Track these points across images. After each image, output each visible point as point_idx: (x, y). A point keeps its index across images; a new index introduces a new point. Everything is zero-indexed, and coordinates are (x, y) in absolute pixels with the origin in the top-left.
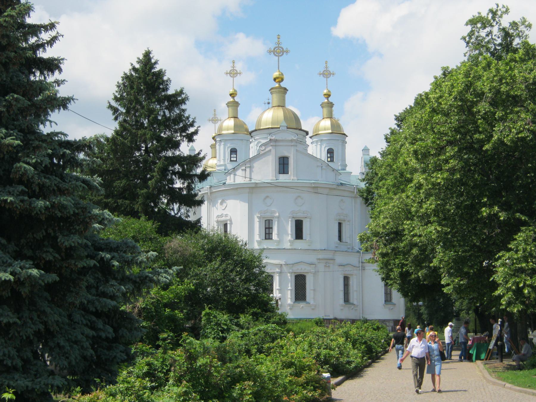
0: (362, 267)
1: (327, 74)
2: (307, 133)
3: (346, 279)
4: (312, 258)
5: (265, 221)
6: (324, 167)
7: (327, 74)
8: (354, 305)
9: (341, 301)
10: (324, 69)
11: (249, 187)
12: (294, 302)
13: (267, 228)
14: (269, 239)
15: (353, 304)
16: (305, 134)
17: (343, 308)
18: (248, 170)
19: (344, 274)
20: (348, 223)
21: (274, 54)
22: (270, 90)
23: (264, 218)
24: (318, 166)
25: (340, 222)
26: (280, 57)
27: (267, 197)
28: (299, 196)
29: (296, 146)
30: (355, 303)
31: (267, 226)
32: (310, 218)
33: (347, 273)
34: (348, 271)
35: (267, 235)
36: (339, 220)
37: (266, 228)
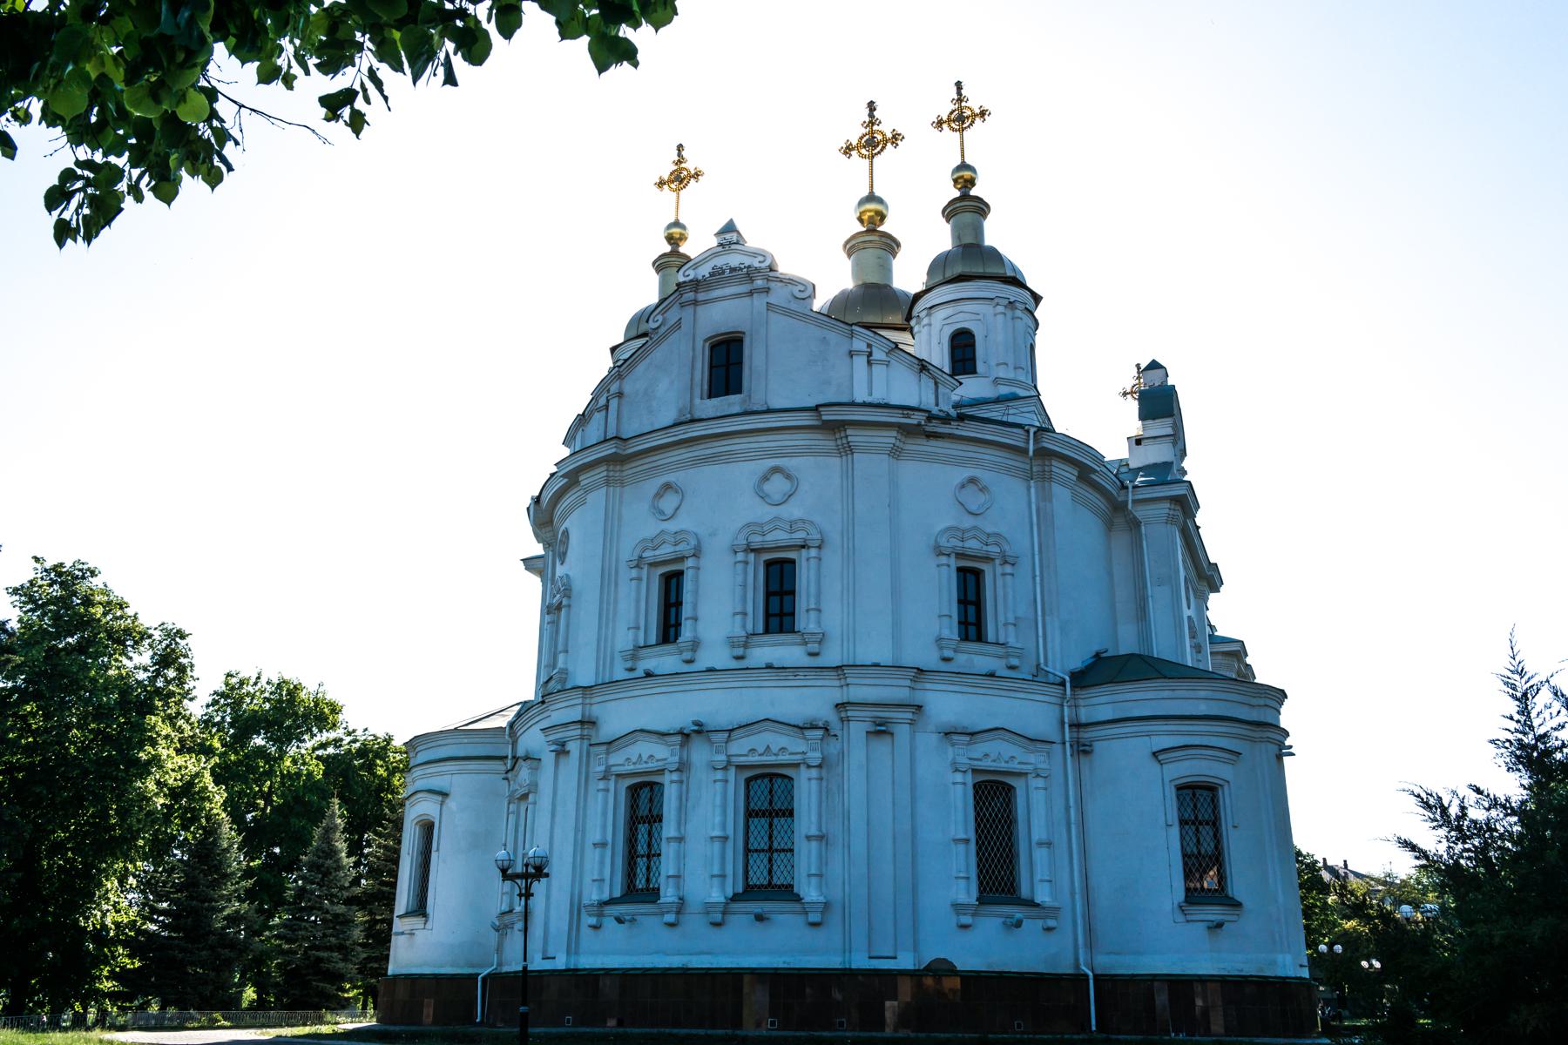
4: (814, 701)
6: (878, 354)
8: (1038, 905)
9: (967, 892)
10: (953, 107)
15: (1031, 903)
17: (966, 920)
18: (614, 404)
20: (1008, 569)
27: (668, 487)
28: (776, 470)
30: (1043, 896)
32: (819, 547)
34: (998, 755)
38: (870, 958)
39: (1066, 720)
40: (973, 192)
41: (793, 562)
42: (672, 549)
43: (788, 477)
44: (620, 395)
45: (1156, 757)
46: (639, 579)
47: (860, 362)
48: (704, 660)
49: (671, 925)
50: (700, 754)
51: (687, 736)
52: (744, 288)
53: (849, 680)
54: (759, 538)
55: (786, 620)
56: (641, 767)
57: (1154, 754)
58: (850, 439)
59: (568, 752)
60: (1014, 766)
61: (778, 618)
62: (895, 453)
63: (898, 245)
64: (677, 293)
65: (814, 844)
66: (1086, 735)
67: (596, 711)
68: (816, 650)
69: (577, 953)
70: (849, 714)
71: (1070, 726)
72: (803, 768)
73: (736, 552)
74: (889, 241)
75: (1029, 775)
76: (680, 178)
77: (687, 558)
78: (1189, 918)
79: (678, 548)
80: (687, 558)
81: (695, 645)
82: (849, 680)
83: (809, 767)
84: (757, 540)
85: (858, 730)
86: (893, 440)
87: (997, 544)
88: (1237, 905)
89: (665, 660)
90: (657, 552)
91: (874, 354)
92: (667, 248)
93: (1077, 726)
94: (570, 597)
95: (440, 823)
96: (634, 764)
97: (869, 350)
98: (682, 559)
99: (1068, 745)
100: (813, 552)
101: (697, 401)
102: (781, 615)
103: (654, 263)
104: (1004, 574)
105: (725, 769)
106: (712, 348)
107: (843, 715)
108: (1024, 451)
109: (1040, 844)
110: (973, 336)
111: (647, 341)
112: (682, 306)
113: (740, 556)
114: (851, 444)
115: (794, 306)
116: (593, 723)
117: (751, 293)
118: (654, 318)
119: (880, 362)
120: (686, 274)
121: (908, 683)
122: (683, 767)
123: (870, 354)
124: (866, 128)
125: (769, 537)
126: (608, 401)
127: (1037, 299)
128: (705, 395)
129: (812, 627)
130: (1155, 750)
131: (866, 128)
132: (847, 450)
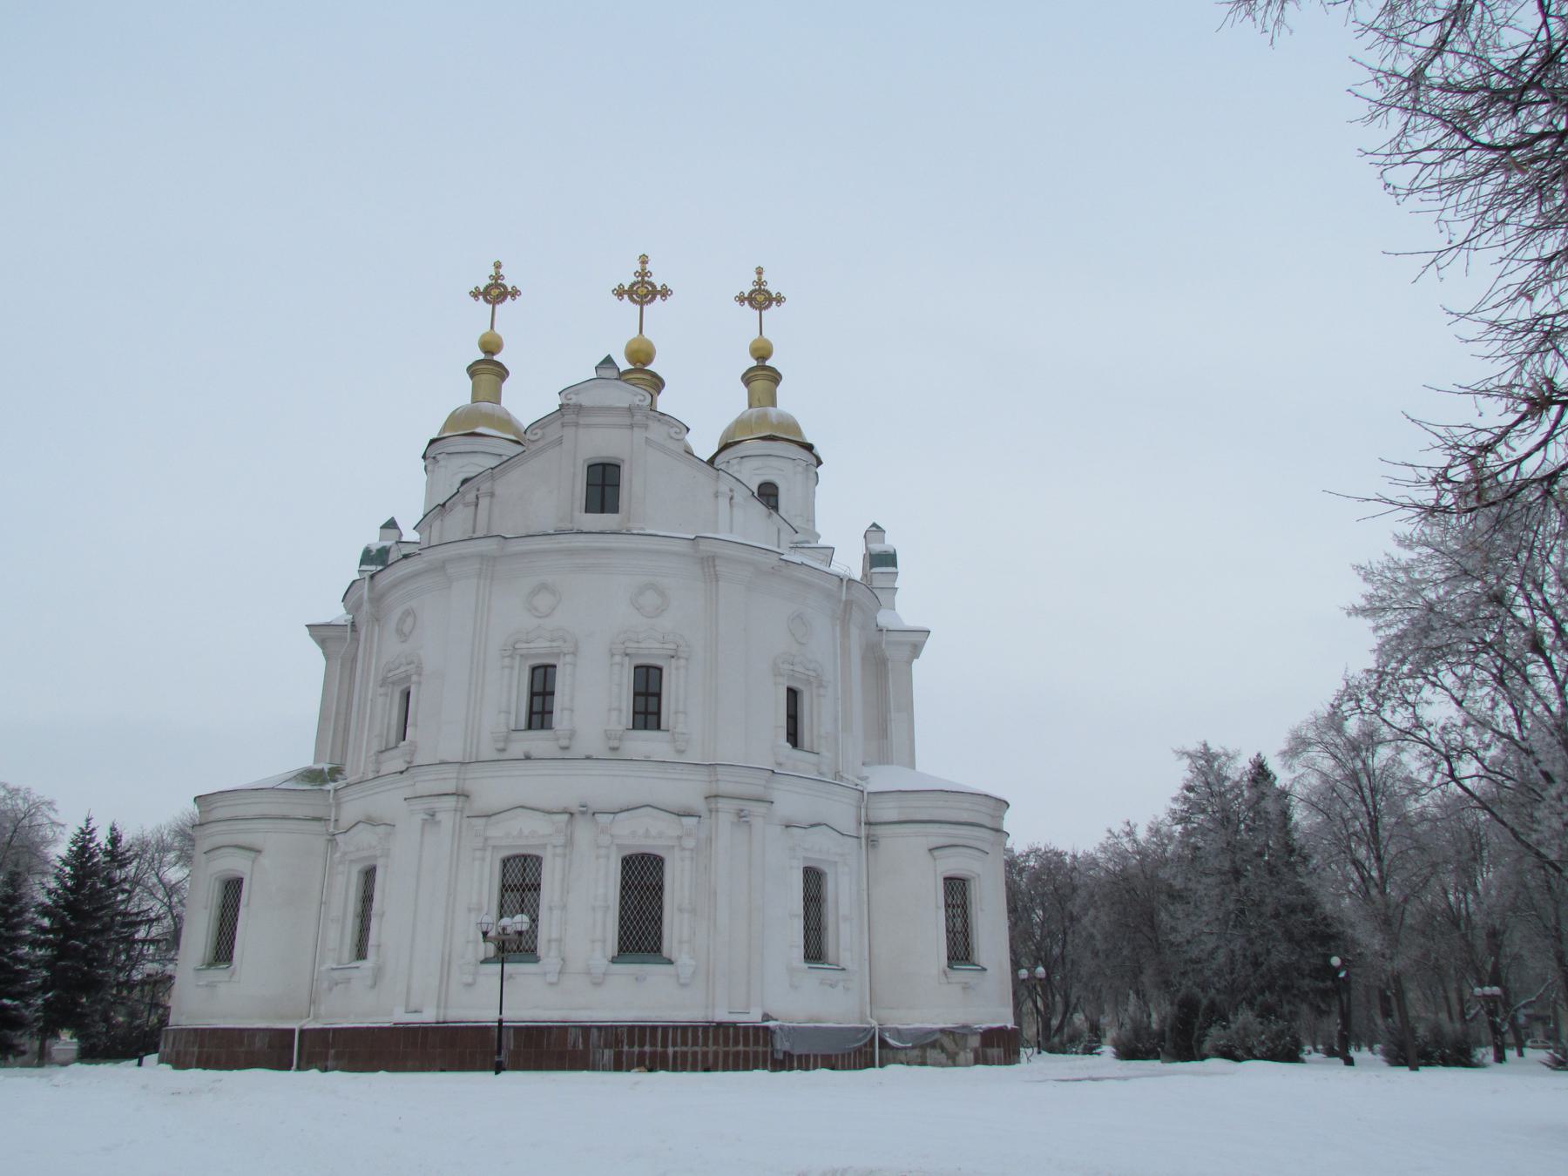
0: (867, 837)
1: (760, 298)
3: (813, 880)
4: (689, 791)
6: (738, 499)
7: (760, 298)
11: (482, 557)
12: (614, 961)
13: (538, 694)
18: (484, 502)
19: (805, 858)
25: (794, 685)
27: (543, 587)
29: (646, 427)
31: (538, 688)
32: (687, 659)
34: (821, 848)
37: (533, 694)
38: (730, 1013)
39: (863, 819)
40: (768, 363)
41: (660, 669)
42: (548, 644)
44: (492, 495)
45: (931, 854)
46: (512, 668)
47: (723, 503)
48: (580, 749)
49: (551, 984)
50: (584, 832)
51: (572, 814)
54: (636, 645)
55: (652, 719)
57: (930, 850)
59: (440, 822)
61: (643, 716)
63: (663, 385)
64: (559, 413)
66: (879, 830)
67: (469, 786)
68: (683, 748)
69: (446, 1007)
71: (866, 824)
73: (613, 655)
74: (657, 381)
76: (496, 292)
78: (950, 981)
79: (554, 644)
80: (565, 654)
81: (572, 735)
82: (719, 777)
83: (683, 849)
85: (725, 819)
88: (984, 969)
89: (538, 741)
90: (532, 645)
91: (735, 497)
92: (482, 356)
93: (868, 824)
94: (420, 675)
95: (251, 879)
98: (558, 655)
99: (863, 840)
100: (682, 662)
101: (577, 514)
102: (646, 713)
103: (469, 368)
105: (608, 847)
106: (589, 467)
107: (713, 806)
110: (777, 488)
111: (524, 451)
112: (563, 425)
113: (617, 659)
116: (467, 796)
118: (534, 430)
120: (569, 397)
122: (569, 843)
123: (731, 498)
124: (637, 277)
125: (642, 645)
126: (477, 498)
127: (819, 463)
128: (584, 510)
130: (931, 847)
131: (637, 277)
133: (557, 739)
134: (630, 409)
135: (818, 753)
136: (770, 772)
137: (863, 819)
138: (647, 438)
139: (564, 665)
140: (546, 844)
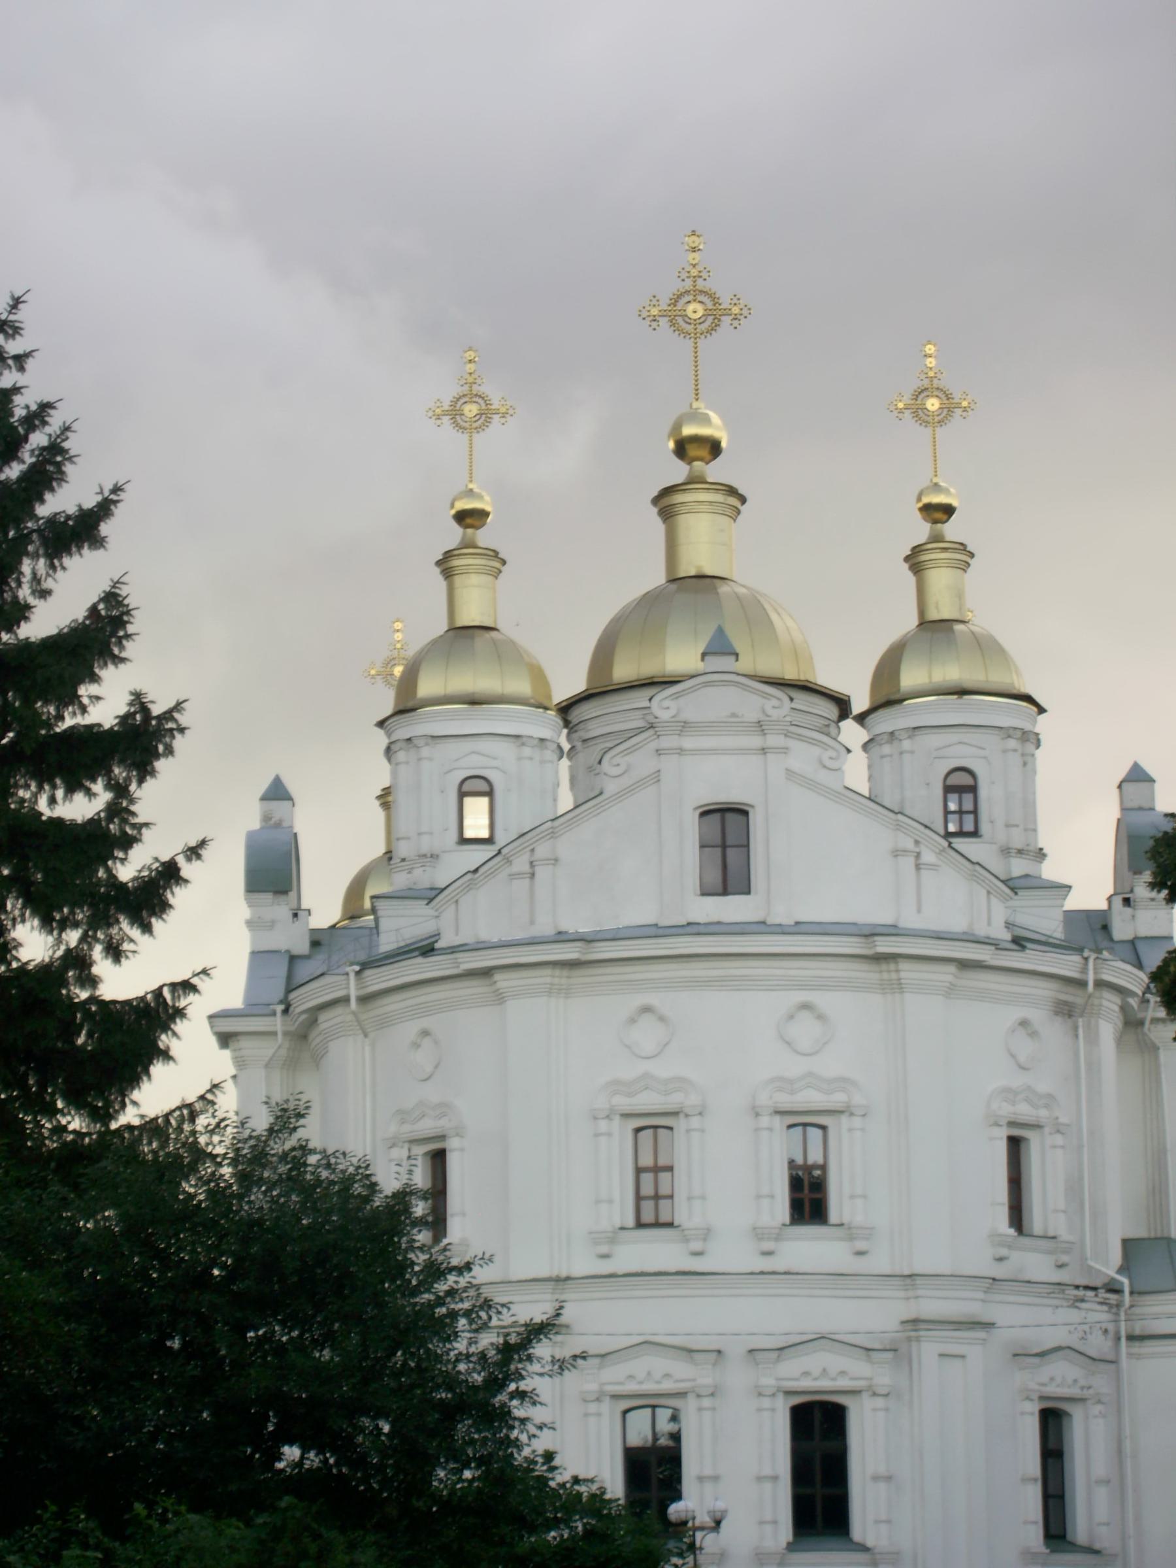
2: (842, 705)
5: (638, 1130)
6: (928, 857)
8: (1097, 1552)
9: (1034, 1535)
14: (657, 1224)
16: (832, 711)
19: (1042, 1398)
20: (1059, 1140)
21: (672, 323)
22: (656, 501)
23: (626, 1116)
24: (897, 853)
25: (1016, 1132)
26: (701, 343)
27: (647, 1009)
28: (806, 1006)
29: (785, 750)
31: (647, 1160)
33: (1052, 1390)
35: (648, 1207)
36: (1012, 1124)
37: (639, 1171)
39: (1123, 1334)
43: (821, 1017)
52: (756, 741)
53: (920, 1292)
56: (649, 1387)
58: (903, 975)
60: (1074, 1392)
62: (950, 991)
65: (882, 1486)
70: (922, 1333)
72: (865, 1395)
73: (757, 1115)
75: (1089, 1402)
77: (687, 1116)
80: (687, 1116)
83: (875, 1394)
84: (785, 1100)
86: (950, 978)
87: (1047, 1106)
96: (641, 1383)
97: (917, 850)
98: (675, 1114)
104: (1054, 1147)
108: (1082, 984)
109: (1099, 1482)
113: (765, 1121)
114: (903, 981)
115: (823, 776)
117: (764, 751)
119: (933, 867)
121: (981, 1295)
123: (918, 855)
129: (859, 1219)
132: (899, 987)
133: (686, 1240)
134: (759, 723)
135: (1054, 1238)
136: (991, 1281)
137: (1123, 1334)
138: (787, 770)
139: (688, 1131)
140: (686, 1393)
